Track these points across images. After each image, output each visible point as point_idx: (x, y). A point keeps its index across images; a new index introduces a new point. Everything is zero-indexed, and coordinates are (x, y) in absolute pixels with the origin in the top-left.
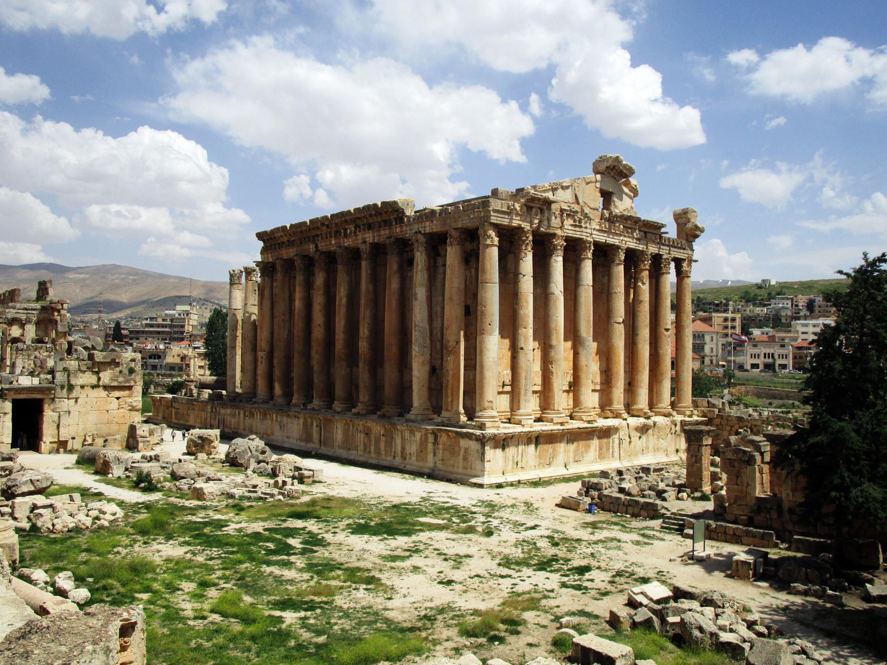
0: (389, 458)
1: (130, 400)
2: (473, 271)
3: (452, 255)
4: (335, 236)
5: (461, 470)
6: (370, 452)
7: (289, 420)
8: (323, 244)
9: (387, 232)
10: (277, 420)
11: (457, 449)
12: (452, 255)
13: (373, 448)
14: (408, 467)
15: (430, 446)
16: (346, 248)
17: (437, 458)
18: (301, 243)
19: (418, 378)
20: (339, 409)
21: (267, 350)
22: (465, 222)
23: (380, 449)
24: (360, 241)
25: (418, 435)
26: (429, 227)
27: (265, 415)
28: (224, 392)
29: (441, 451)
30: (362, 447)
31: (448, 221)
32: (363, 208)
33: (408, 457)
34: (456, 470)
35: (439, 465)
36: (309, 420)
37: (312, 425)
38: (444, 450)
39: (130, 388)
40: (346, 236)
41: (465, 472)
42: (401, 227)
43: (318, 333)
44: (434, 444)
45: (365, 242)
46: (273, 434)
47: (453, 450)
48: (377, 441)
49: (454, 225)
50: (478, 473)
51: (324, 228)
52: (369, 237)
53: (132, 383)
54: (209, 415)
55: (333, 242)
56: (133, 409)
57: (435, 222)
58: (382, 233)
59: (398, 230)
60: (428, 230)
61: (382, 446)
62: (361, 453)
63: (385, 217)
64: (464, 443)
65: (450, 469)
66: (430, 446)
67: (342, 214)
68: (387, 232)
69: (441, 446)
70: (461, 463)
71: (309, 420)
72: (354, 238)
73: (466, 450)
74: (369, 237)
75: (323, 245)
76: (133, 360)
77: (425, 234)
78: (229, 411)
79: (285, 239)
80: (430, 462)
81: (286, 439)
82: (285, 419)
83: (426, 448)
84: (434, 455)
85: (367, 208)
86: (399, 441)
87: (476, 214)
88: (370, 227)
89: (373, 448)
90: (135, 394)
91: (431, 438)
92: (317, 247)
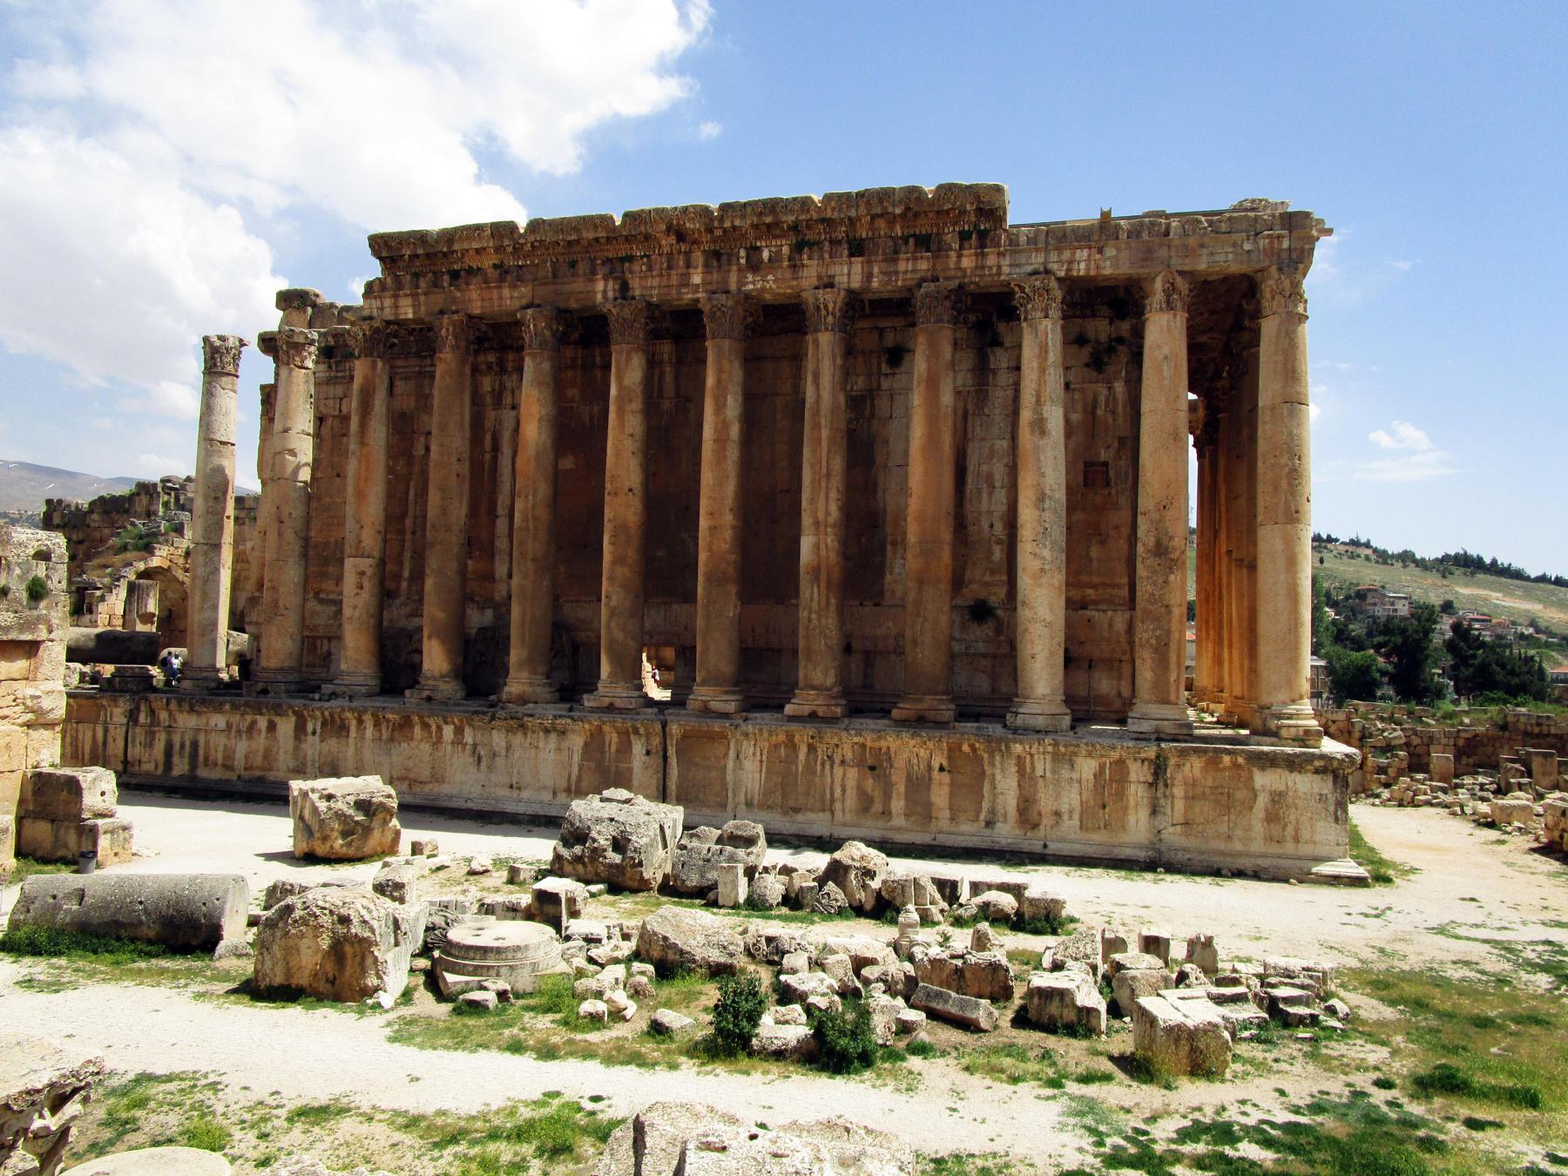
0: (966, 828)
1: (30, 691)
2: (1119, 387)
3: (1165, 336)
4: (706, 265)
5: (1257, 846)
6: (886, 813)
7: (518, 739)
8: (656, 282)
9: (923, 265)
10: (458, 740)
11: (1241, 794)
12: (1165, 336)
13: (898, 805)
14: (1066, 849)
15: (1137, 792)
16: (748, 296)
17: (1161, 822)
18: (555, 276)
19: (1049, 625)
20: (731, 707)
21: (376, 553)
22: (1223, 260)
23: (929, 805)
24: (815, 282)
25: (1087, 767)
26: (1083, 263)
27: (404, 725)
28: (155, 671)
29: (1180, 805)
30: (851, 800)
31: (1162, 253)
32: (860, 195)
33: (1047, 821)
34: (1238, 846)
35: (1173, 836)
36: (612, 738)
37: (625, 749)
38: (1190, 799)
39: (31, 649)
40: (754, 266)
41: (1274, 849)
42: (984, 255)
43: (622, 507)
44: (1152, 785)
45: (831, 285)
46: (438, 779)
47: (1228, 801)
48: (918, 786)
49: (1176, 263)
50: (1323, 851)
51: (672, 239)
52: (850, 273)
53: (42, 634)
54: (118, 733)
55: (697, 279)
56: (38, 721)
57: (1110, 252)
58: (902, 266)
59: (967, 262)
60: (1081, 269)
61: (940, 796)
62: (849, 817)
63: (923, 227)
64: (1265, 780)
65: (1221, 845)
66: (1137, 792)
67: (772, 206)
68: (923, 265)
69: (1178, 791)
70: (1258, 828)
71: (612, 738)
72: (788, 274)
73: (1277, 798)
74: (850, 273)
75: (648, 285)
76: (43, 555)
77: (1059, 279)
78: (219, 720)
79: (488, 262)
80: (1137, 829)
81: (506, 792)
82: (498, 739)
83: (1121, 795)
84: (1154, 812)
85: (884, 195)
86: (1006, 786)
87: (1263, 243)
88: (857, 248)
89: (898, 805)
90: (46, 669)
91: (1138, 773)
92: (624, 288)
